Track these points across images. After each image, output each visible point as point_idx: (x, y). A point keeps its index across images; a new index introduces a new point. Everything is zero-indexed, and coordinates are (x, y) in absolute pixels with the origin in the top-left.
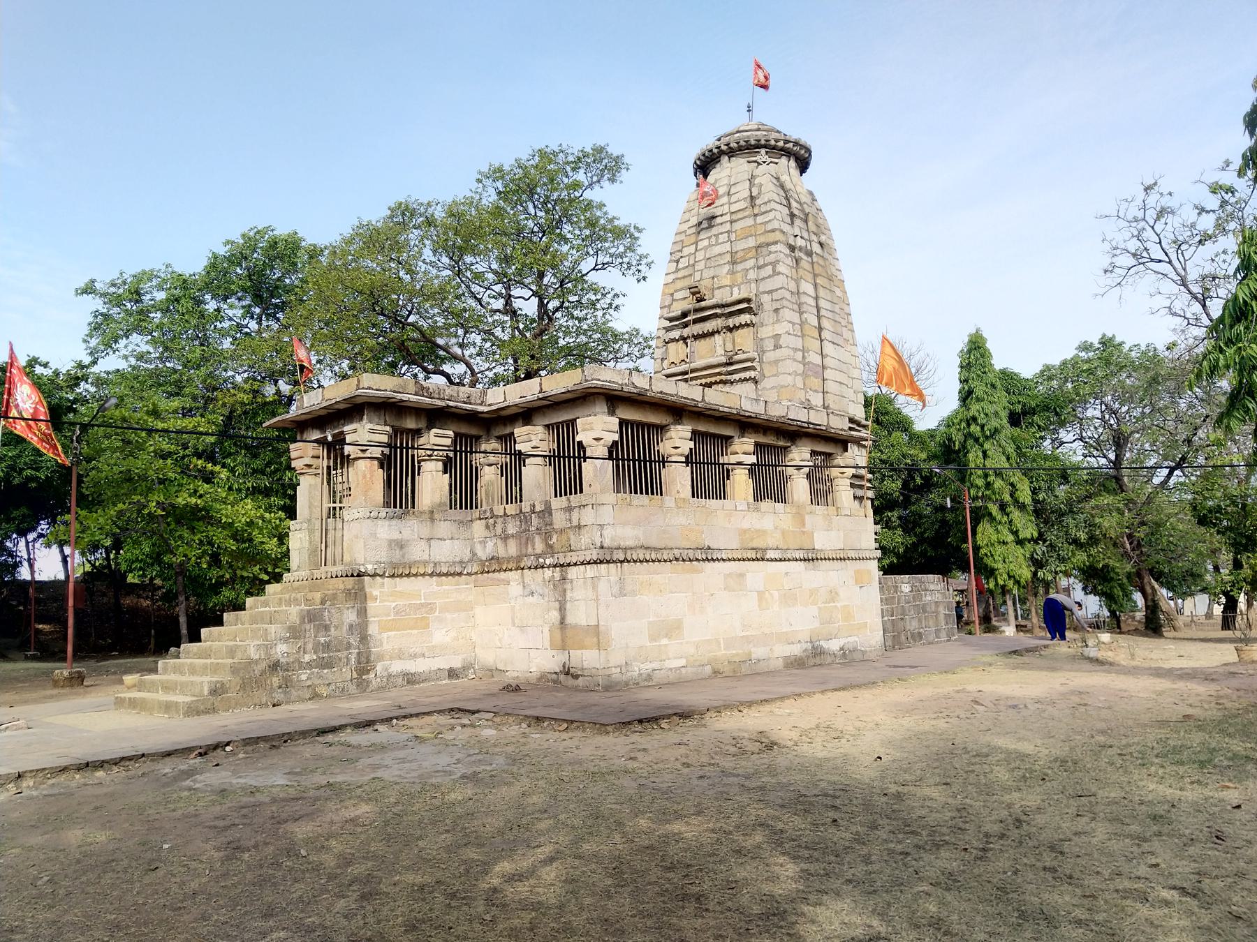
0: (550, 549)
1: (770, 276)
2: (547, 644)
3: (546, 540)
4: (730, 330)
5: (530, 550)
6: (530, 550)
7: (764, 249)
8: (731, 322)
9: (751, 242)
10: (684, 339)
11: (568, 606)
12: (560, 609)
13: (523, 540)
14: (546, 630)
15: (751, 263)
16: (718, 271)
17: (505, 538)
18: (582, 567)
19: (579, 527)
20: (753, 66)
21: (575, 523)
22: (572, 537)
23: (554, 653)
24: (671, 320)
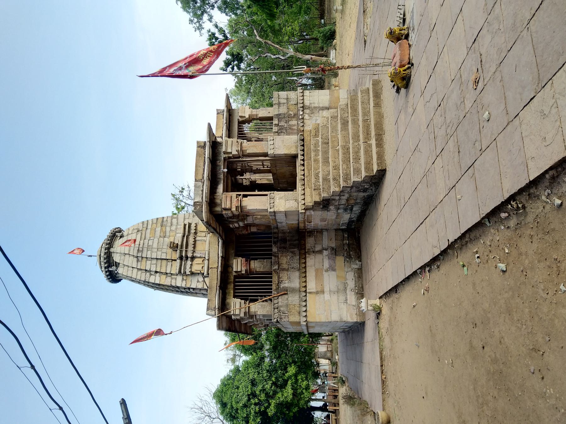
0: (296, 115)
3: (292, 117)
4: (196, 233)
5: (295, 127)
6: (295, 127)
8: (193, 231)
10: (193, 258)
11: (321, 105)
12: (323, 110)
13: (291, 131)
18: (305, 97)
19: (287, 99)
20: (71, 255)
21: (285, 101)
22: (292, 103)
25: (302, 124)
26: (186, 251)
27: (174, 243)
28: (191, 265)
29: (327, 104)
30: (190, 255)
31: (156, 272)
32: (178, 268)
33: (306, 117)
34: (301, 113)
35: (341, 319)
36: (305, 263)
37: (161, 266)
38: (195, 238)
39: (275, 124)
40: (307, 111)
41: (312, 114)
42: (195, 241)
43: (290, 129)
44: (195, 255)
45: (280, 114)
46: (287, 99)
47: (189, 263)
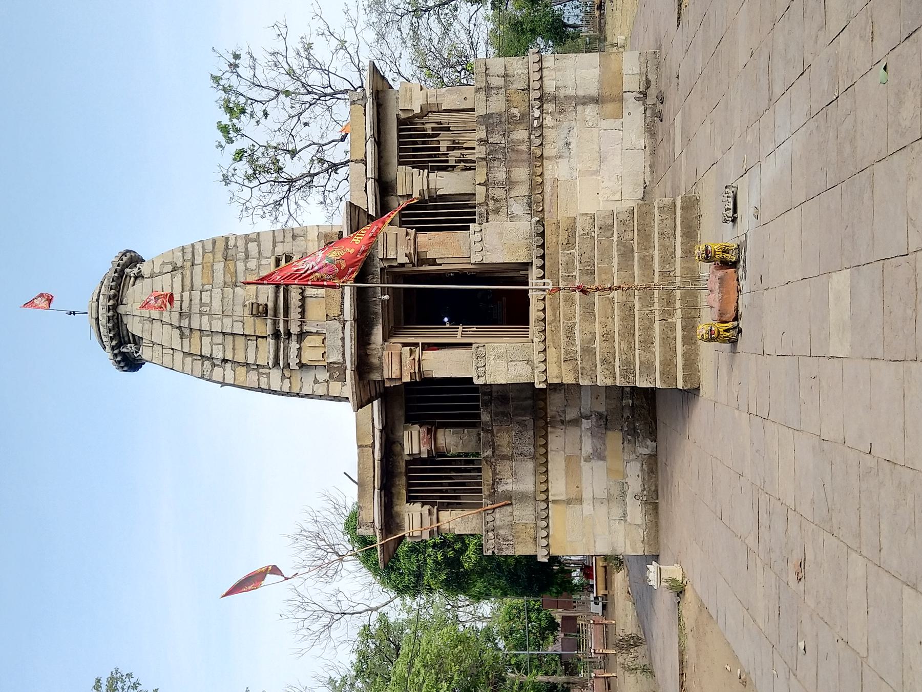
0: (525, 117)
1: (259, 246)
2: (619, 122)
6: (524, 147)
7: (230, 252)
9: (219, 266)
10: (302, 336)
11: (581, 93)
12: (584, 104)
13: (513, 156)
14: (604, 124)
15: (240, 266)
16: (239, 301)
17: (510, 183)
18: (545, 72)
19: (506, 76)
21: (500, 82)
22: (515, 86)
23: (625, 114)
24: (276, 363)
25: (538, 142)
26: (286, 322)
27: (259, 305)
28: (300, 349)
29: (593, 91)
30: (294, 329)
31: (225, 361)
32: (272, 356)
33: (548, 121)
34: (537, 113)
35: (614, 549)
36: (545, 445)
37: (234, 349)
38: (302, 294)
39: (481, 140)
40: (550, 107)
41: (561, 112)
42: (303, 299)
43: (513, 150)
44: (305, 328)
45: (490, 116)
46: (506, 76)
47: (294, 345)
